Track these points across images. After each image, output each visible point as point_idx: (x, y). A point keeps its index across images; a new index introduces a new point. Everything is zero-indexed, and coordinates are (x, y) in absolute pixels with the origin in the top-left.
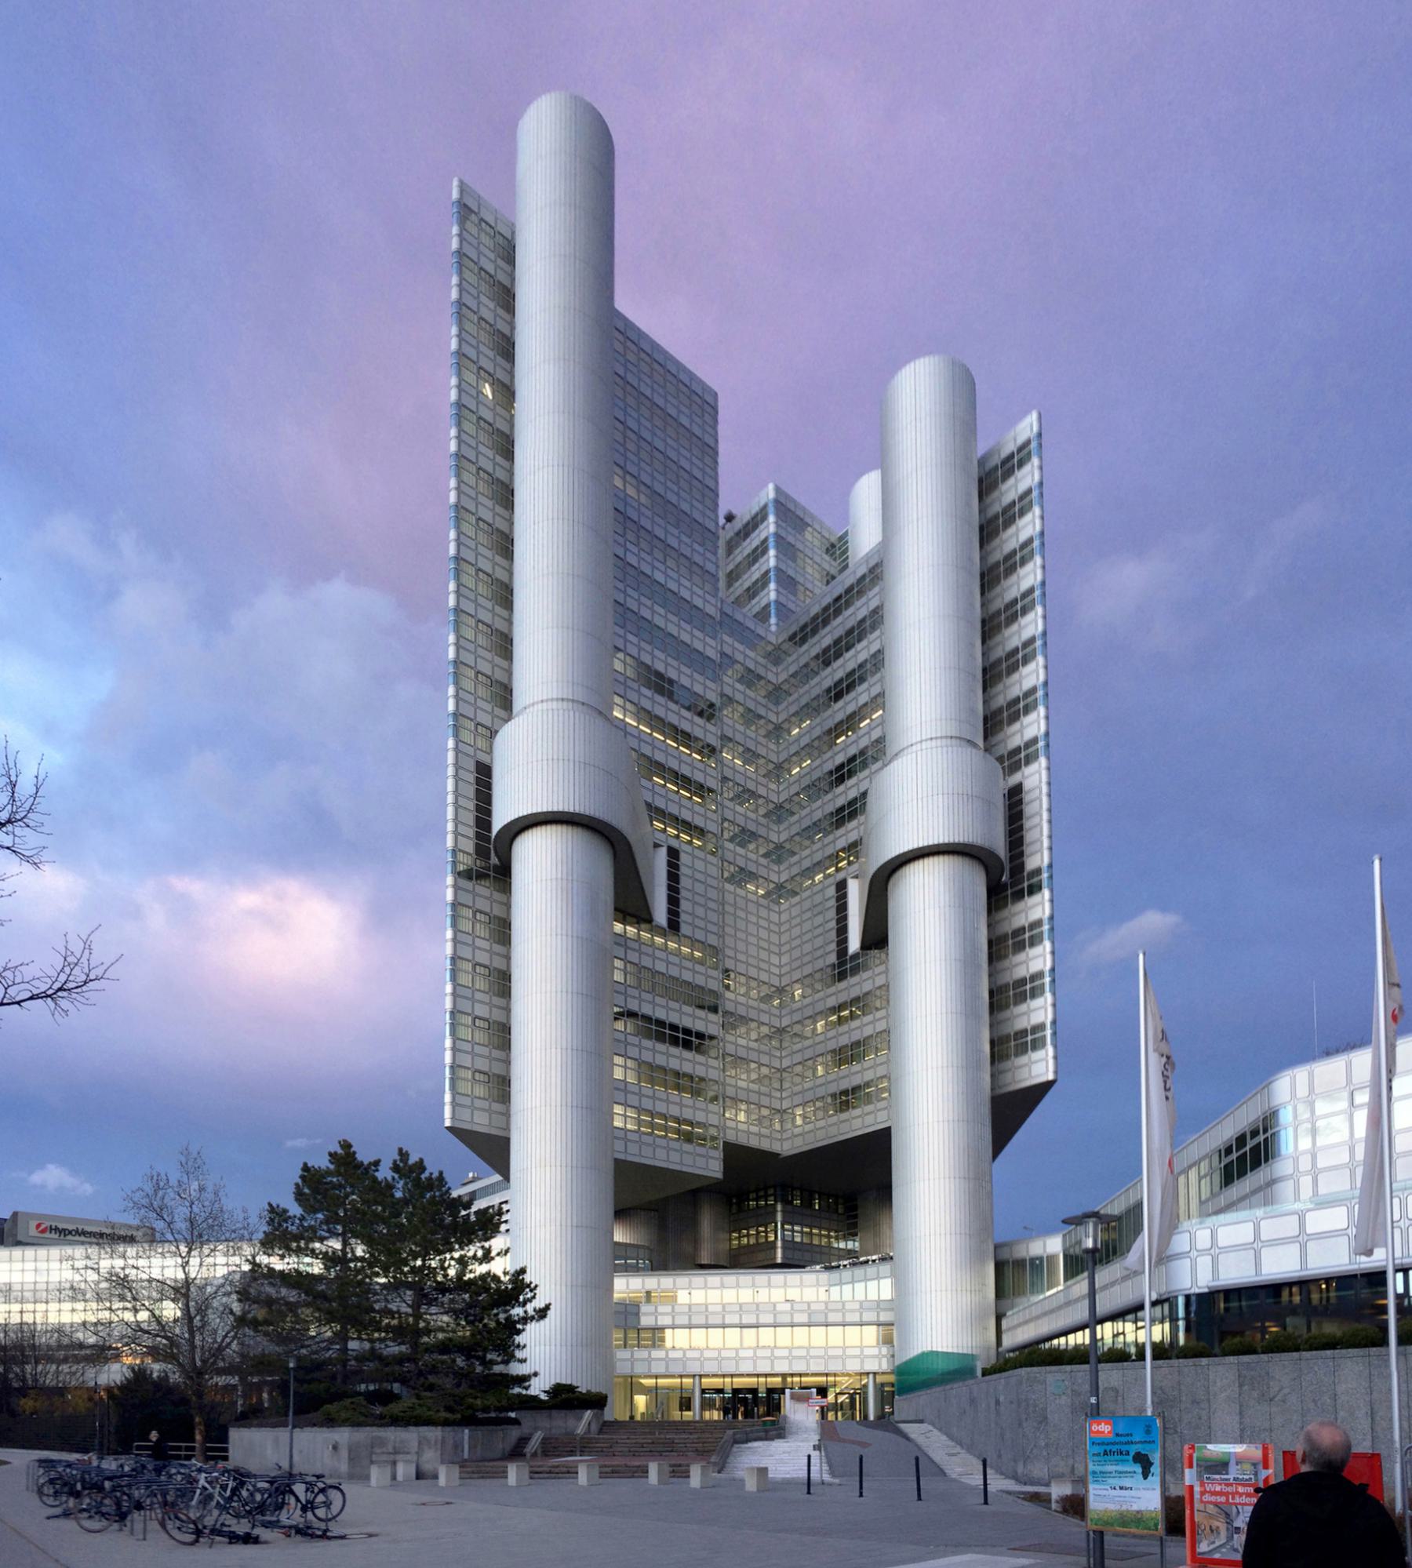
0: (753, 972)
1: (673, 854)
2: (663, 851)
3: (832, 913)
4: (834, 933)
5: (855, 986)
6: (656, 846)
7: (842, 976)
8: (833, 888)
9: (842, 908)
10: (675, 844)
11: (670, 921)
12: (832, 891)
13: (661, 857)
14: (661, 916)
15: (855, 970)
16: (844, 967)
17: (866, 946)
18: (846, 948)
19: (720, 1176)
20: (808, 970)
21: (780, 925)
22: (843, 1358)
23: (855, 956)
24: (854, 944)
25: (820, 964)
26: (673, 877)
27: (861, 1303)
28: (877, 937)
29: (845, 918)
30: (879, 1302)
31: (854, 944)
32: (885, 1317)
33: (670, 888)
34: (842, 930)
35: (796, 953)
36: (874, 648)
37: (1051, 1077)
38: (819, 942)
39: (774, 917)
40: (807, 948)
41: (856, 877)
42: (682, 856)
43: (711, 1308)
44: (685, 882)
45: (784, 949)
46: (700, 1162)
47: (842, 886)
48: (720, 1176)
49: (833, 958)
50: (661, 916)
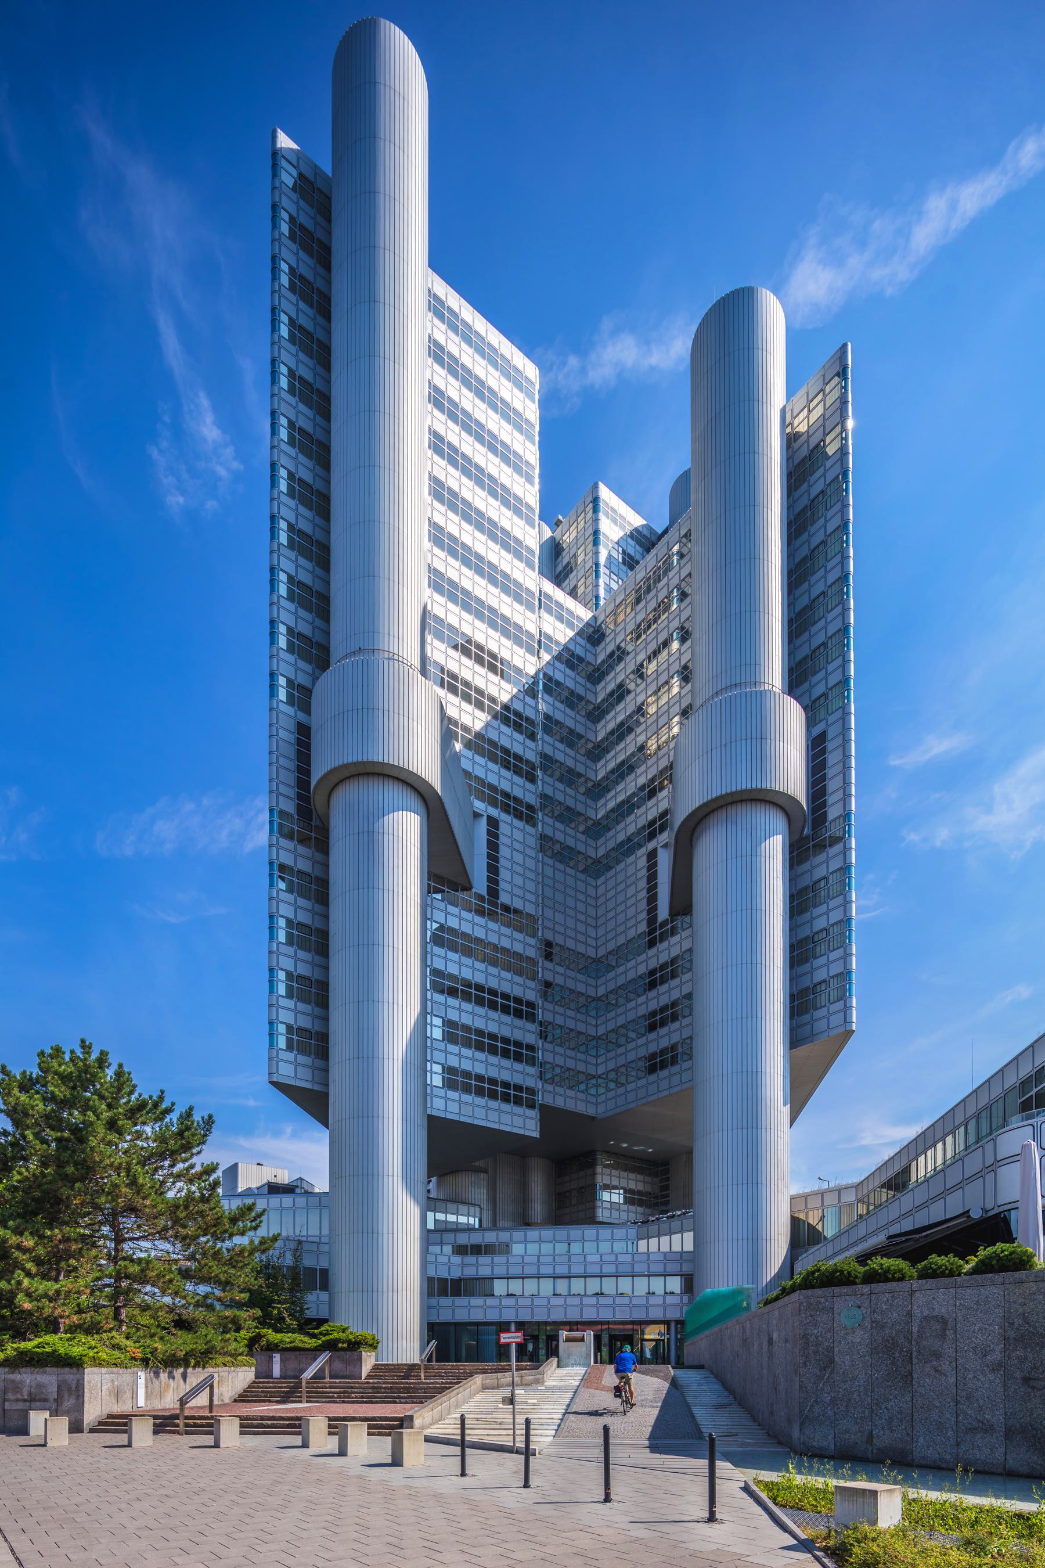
1: (493, 822)
2: (484, 822)
4: (645, 901)
8: (645, 858)
10: (494, 812)
14: (480, 885)
17: (674, 913)
22: (647, 1307)
23: (664, 923)
24: (663, 914)
26: (493, 846)
27: (665, 1254)
28: (683, 905)
29: (656, 886)
30: (682, 1253)
32: (686, 1268)
39: (591, 891)
41: (665, 846)
42: (502, 825)
43: (527, 1259)
45: (600, 922)
47: (652, 855)
49: (643, 927)
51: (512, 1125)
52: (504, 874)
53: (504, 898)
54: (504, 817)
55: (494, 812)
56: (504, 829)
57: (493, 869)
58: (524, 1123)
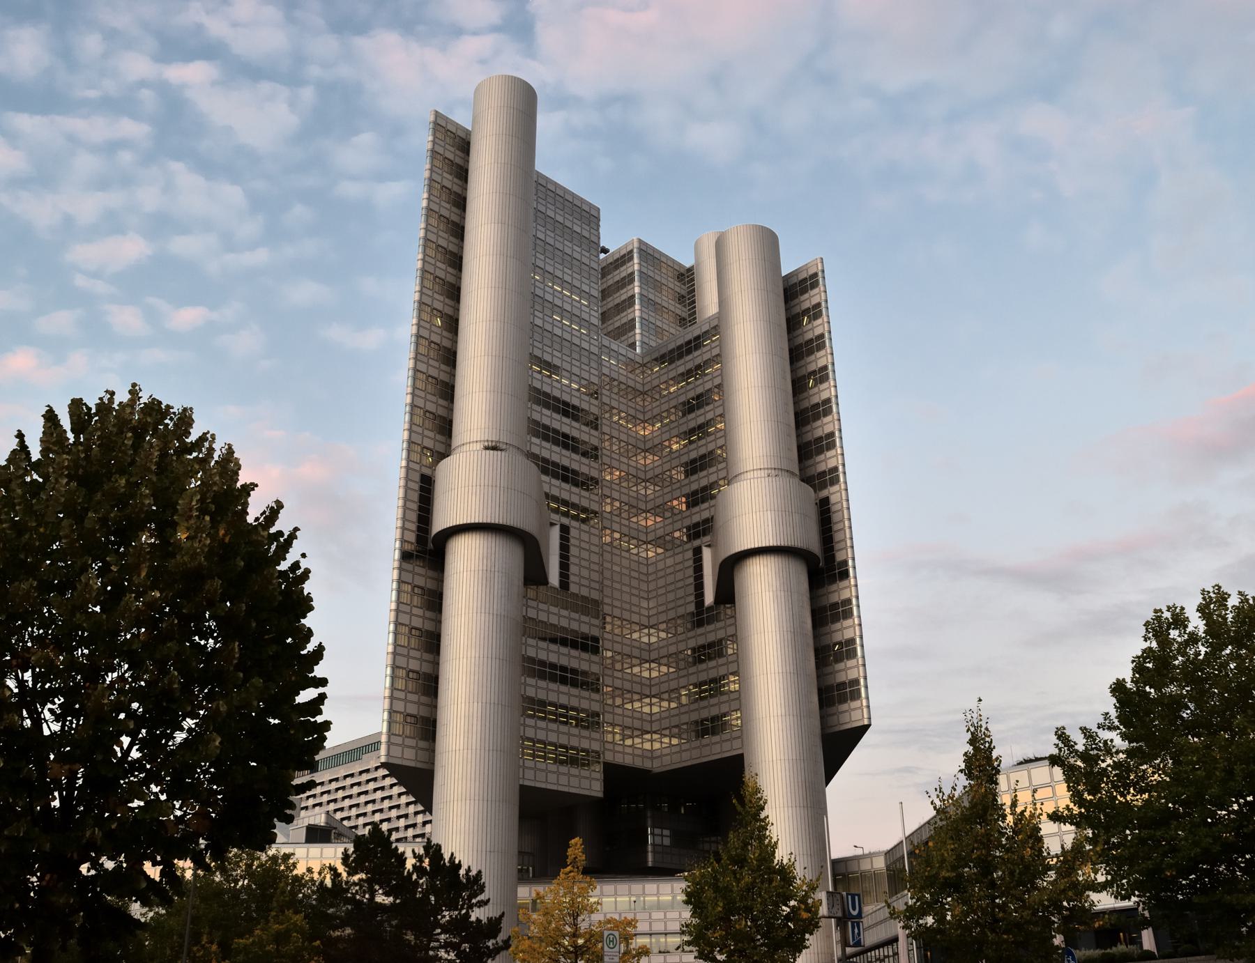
0: (626, 615)
1: (565, 530)
3: (690, 572)
5: (710, 633)
6: (552, 524)
7: (700, 624)
9: (698, 569)
10: (565, 521)
11: (561, 582)
12: (690, 554)
13: (555, 533)
14: (554, 578)
15: (710, 621)
16: (701, 616)
18: (703, 601)
19: (600, 795)
20: (672, 614)
21: (647, 574)
23: (710, 608)
24: (709, 599)
25: (681, 611)
31: (709, 599)
33: (562, 556)
34: (699, 586)
35: (662, 600)
36: (706, 515)
37: (866, 722)
38: (680, 593)
40: (671, 597)
41: (709, 546)
44: (573, 551)
46: (585, 783)
47: (698, 552)
48: (600, 795)
50: (554, 578)
51: (580, 787)
52: (573, 569)
53: (573, 588)
54: (574, 524)
55: (565, 521)
56: (573, 533)
57: (564, 566)
58: (590, 784)
